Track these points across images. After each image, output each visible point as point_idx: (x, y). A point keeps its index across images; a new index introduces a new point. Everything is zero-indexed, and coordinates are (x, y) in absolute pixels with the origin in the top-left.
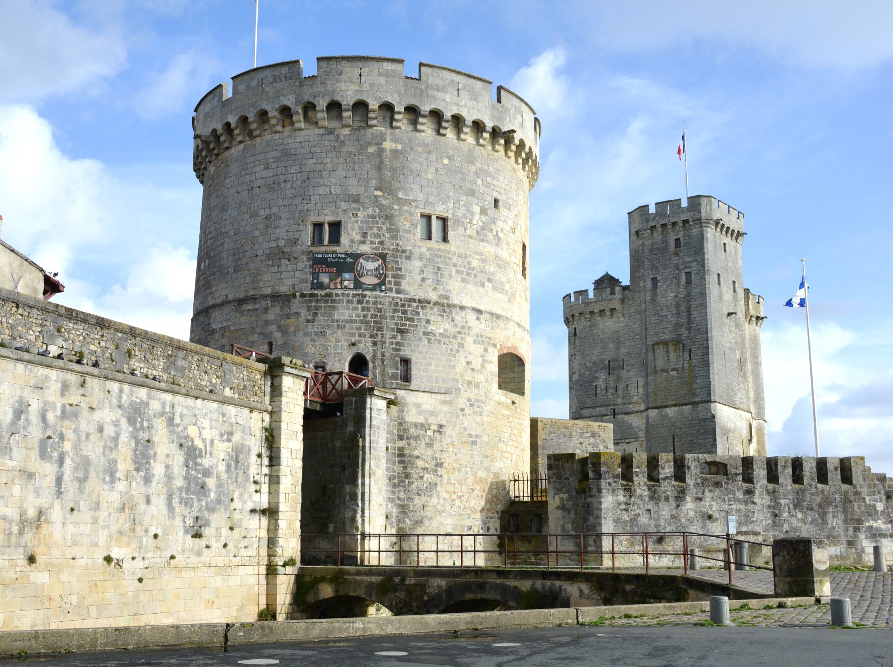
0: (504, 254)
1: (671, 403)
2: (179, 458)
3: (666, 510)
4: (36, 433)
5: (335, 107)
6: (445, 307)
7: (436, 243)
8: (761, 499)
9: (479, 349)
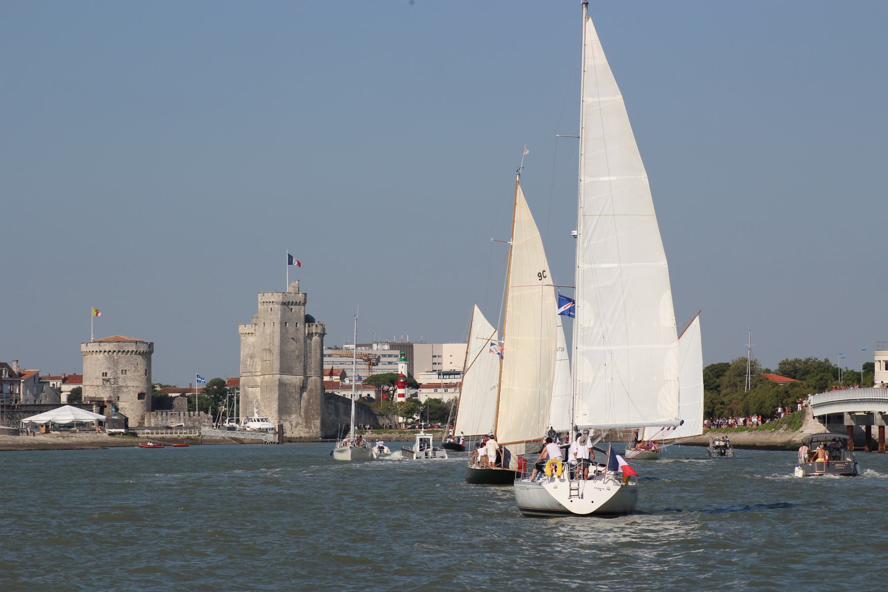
6: (127, 387)
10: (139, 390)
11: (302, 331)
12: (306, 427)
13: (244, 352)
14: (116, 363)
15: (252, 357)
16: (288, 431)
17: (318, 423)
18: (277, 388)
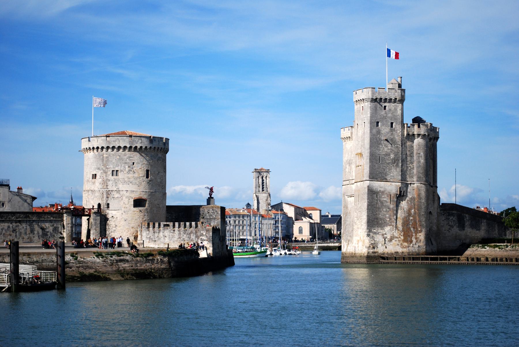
0: (136, 175)
1: (359, 180)
2: (41, 230)
3: (156, 235)
4: (11, 229)
5: (93, 148)
6: (118, 191)
7: (115, 177)
8: (177, 232)
9: (127, 199)
10: (136, 196)
11: (399, 131)
12: (405, 240)
13: (346, 158)
14: (105, 162)
15: (350, 164)
16: (380, 245)
17: (422, 236)
18: (366, 196)
